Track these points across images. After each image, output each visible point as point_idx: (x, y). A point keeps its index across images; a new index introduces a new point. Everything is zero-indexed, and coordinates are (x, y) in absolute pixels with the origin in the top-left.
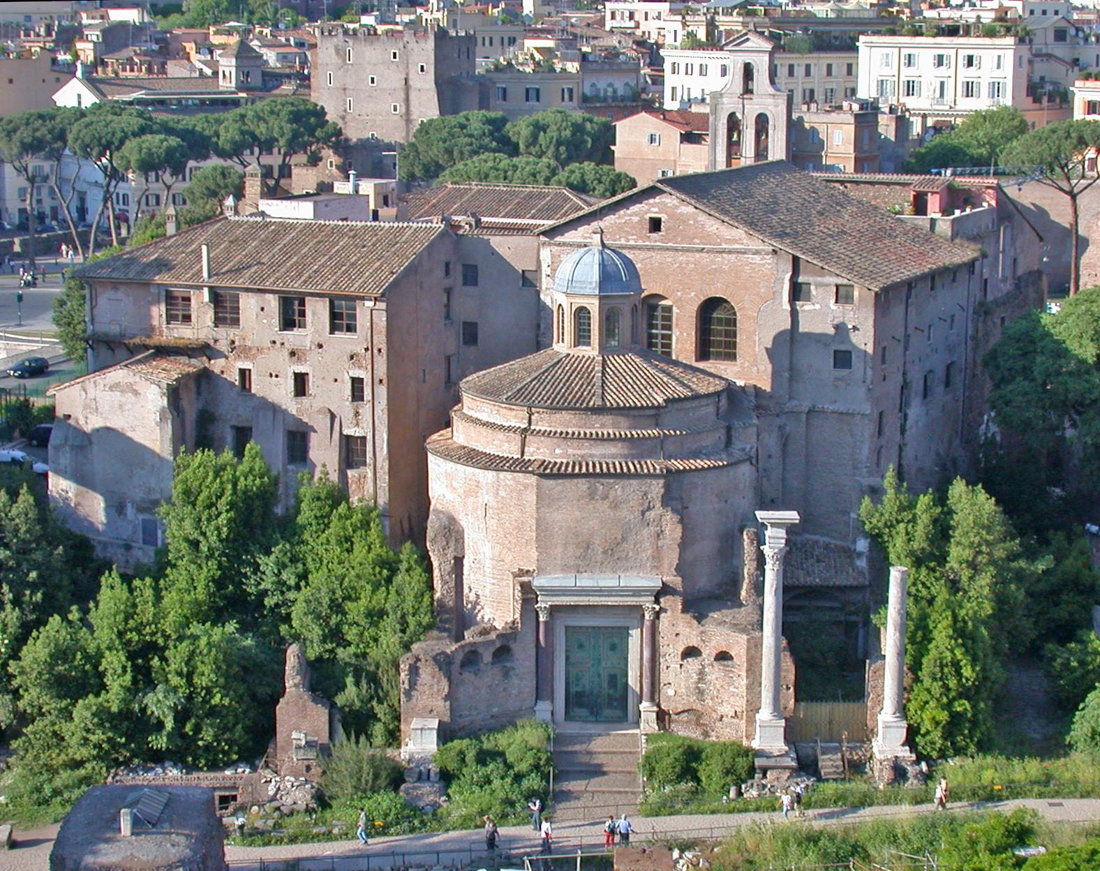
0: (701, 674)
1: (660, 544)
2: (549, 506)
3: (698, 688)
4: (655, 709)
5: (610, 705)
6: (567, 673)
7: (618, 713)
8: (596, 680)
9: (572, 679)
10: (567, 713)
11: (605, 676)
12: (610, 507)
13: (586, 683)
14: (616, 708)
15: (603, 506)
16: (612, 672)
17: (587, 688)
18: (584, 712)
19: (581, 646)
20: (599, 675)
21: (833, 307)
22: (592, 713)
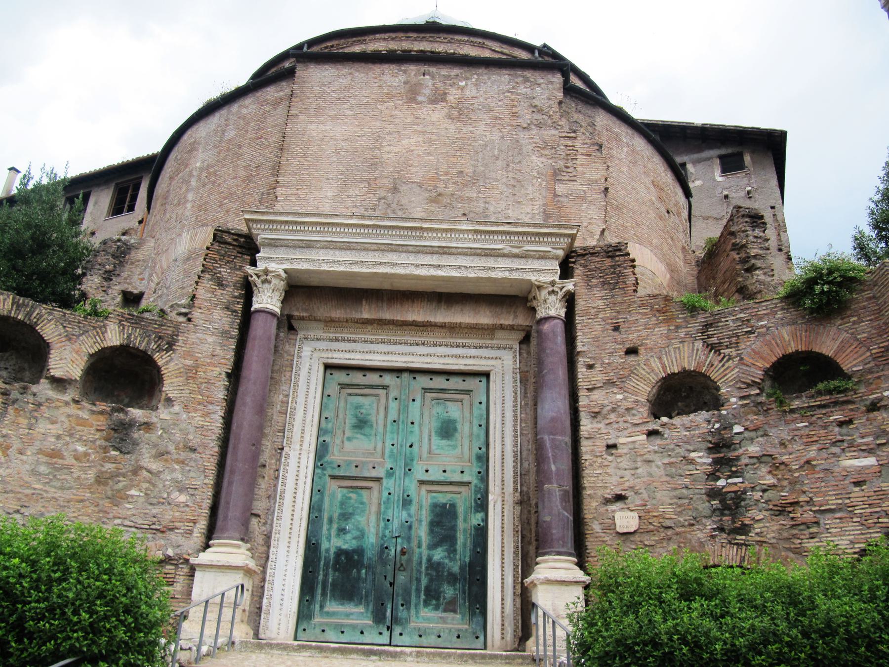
0: (721, 449)
1: (560, 189)
2: (318, 112)
3: (713, 494)
4: (580, 575)
5: (432, 596)
6: (317, 492)
7: (456, 621)
8: (398, 516)
9: (330, 508)
10: (304, 614)
11: (424, 499)
12: (450, 117)
13: (368, 529)
14: (451, 607)
15: (437, 114)
16: (442, 499)
17: (371, 540)
18: (356, 614)
19: (361, 424)
20: (407, 502)
21: (719, 179)
22: (379, 617)
